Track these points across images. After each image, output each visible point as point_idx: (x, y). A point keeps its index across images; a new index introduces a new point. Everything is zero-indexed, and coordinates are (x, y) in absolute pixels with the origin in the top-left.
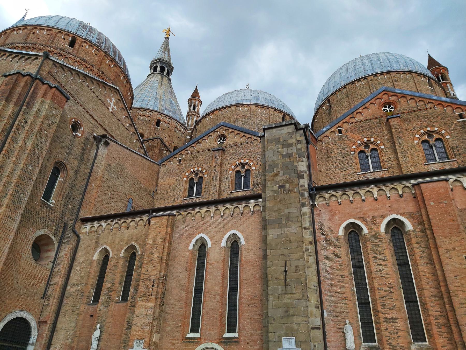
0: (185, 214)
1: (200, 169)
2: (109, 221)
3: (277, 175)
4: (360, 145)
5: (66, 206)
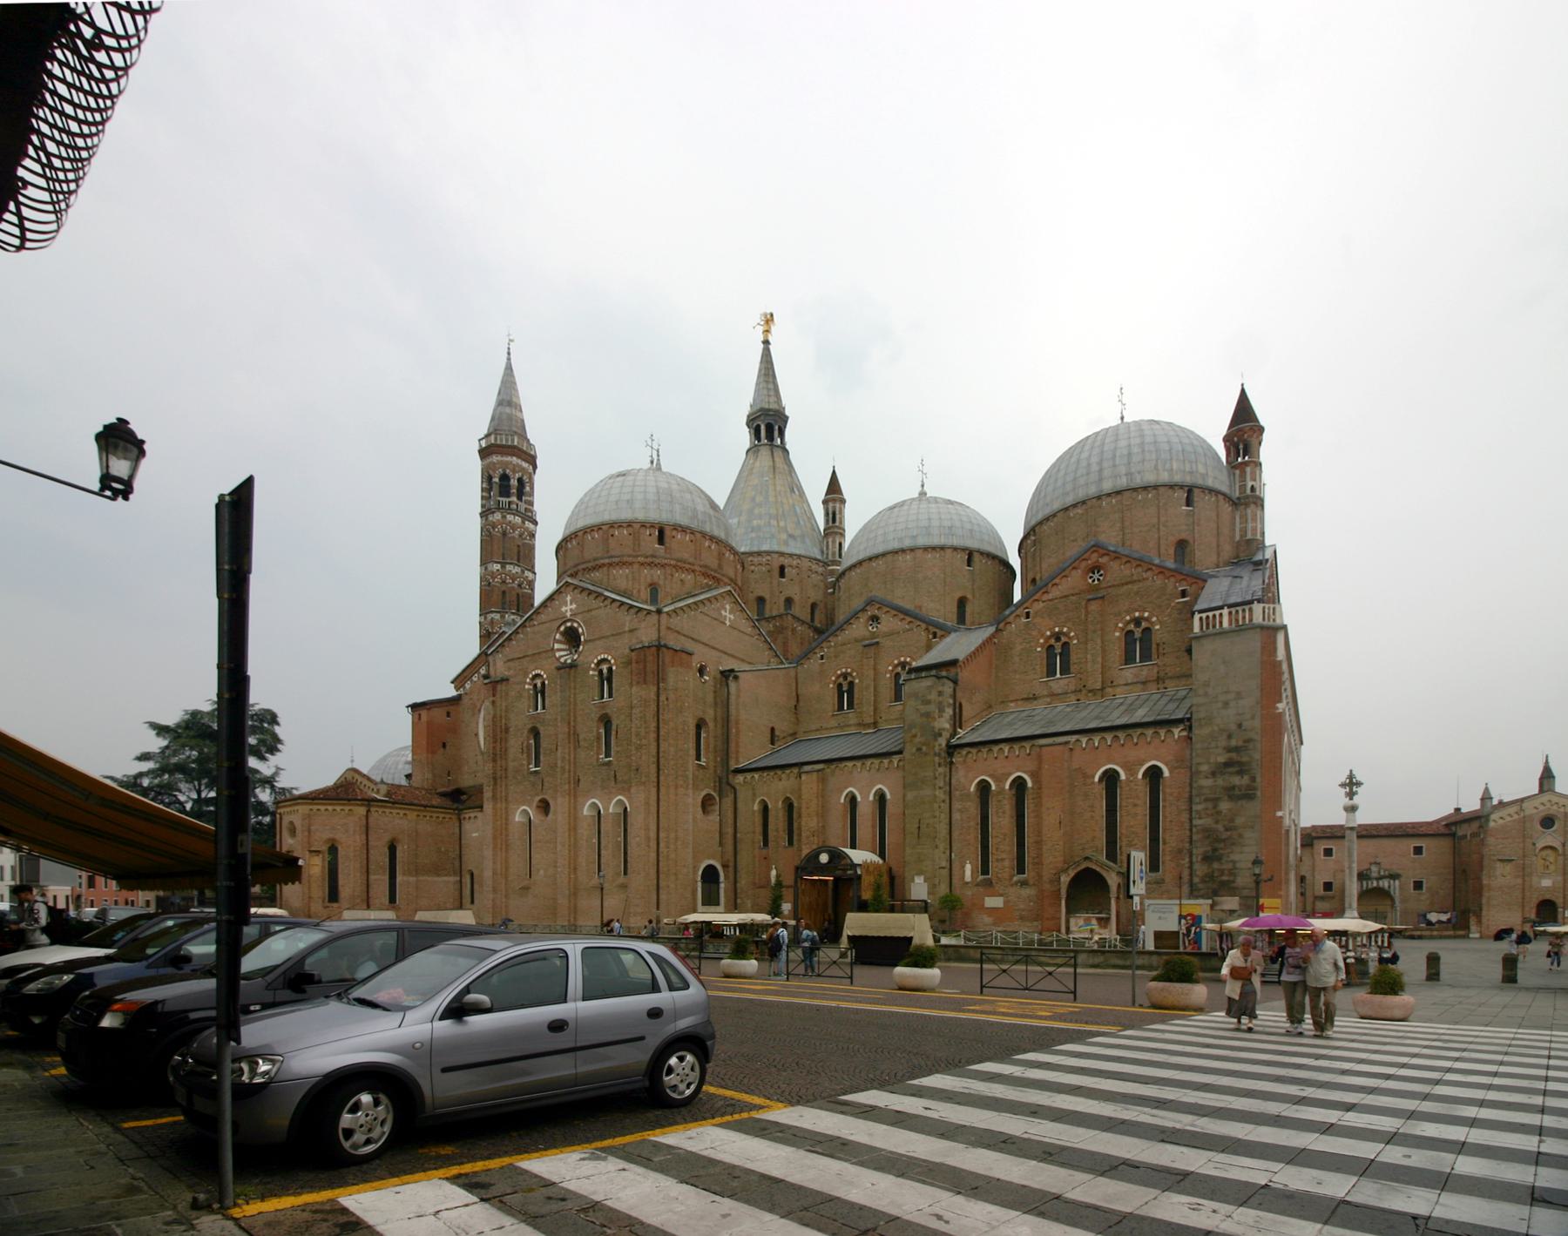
0: (833, 767)
1: (849, 670)
2: (760, 773)
3: (915, 736)
4: (1050, 637)
5: (716, 762)
